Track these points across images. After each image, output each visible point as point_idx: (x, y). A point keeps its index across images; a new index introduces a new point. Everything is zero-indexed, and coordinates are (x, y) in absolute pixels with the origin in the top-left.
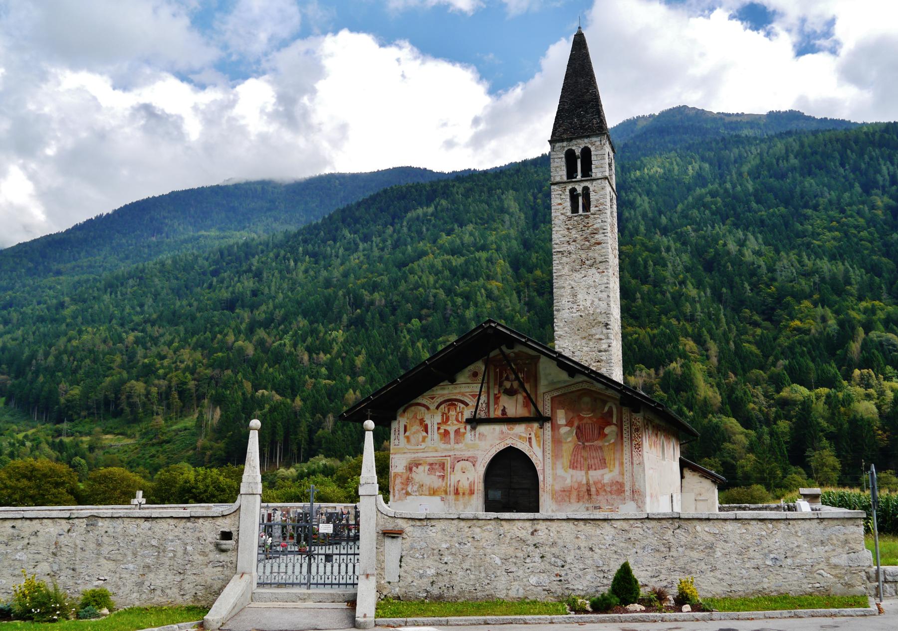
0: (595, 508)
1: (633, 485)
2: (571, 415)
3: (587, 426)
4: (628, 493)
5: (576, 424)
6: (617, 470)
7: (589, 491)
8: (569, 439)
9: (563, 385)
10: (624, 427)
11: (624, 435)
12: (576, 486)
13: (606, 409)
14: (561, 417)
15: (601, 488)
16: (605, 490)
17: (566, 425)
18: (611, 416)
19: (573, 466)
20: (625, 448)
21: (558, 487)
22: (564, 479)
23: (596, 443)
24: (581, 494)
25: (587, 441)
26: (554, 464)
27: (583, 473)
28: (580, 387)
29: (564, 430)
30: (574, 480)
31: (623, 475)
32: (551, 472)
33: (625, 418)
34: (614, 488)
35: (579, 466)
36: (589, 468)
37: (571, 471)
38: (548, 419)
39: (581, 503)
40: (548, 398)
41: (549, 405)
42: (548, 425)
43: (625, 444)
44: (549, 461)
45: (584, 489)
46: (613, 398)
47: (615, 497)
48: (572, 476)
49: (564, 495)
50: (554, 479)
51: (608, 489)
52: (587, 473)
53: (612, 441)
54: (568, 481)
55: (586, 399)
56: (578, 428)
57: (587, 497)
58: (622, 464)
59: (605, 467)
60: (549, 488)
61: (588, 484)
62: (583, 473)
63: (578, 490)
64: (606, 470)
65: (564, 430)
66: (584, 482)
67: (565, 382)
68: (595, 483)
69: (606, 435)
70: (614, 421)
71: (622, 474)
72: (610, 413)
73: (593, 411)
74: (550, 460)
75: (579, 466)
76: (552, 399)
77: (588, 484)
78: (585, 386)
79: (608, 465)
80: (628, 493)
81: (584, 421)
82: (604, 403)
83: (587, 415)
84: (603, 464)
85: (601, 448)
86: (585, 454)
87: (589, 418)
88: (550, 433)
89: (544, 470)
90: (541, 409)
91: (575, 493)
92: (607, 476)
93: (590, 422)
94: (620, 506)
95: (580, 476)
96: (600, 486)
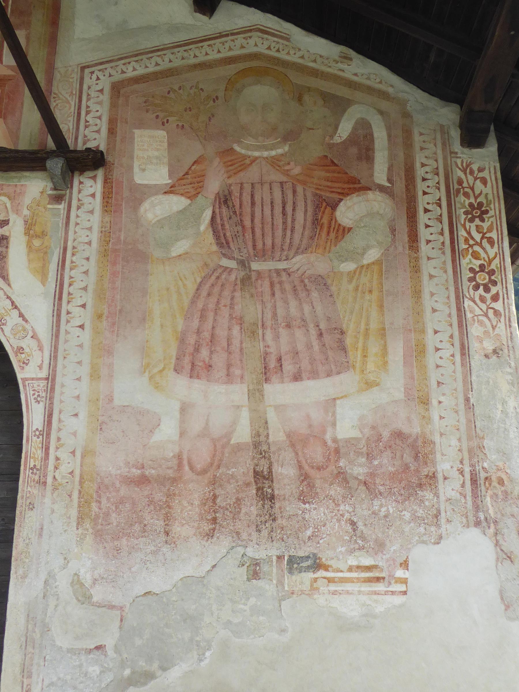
0: (294, 564)
1: (476, 451)
2: (194, 149)
3: (262, 194)
4: (450, 489)
5: (214, 185)
6: (394, 385)
7: (263, 478)
8: (181, 247)
9: (168, 40)
10: (422, 202)
11: (424, 234)
12: (202, 455)
13: (345, 129)
14: (150, 158)
15: (325, 466)
16: (342, 477)
17: (171, 190)
18: (367, 155)
19: (193, 360)
20: (428, 287)
21: (111, 463)
22: (148, 422)
23: (298, 262)
24: (227, 495)
25: (262, 254)
26: (103, 351)
27: (238, 393)
28: (236, 47)
29: (159, 209)
30: (196, 426)
31: (425, 402)
32: (84, 388)
33: (426, 161)
34: (386, 463)
35: (219, 360)
36: (269, 370)
37: (183, 387)
38: (91, 161)
39: (223, 543)
40: (99, 83)
41: (104, 111)
42: (89, 188)
43: (428, 268)
44: (78, 339)
45: (243, 468)
46: (370, 90)
47: (390, 507)
48: (185, 409)
49: (137, 504)
50: (99, 426)
51: (359, 470)
52: (256, 395)
53: (373, 255)
54: (168, 431)
55: (261, 92)
56: (224, 199)
57: (251, 509)
58: (417, 352)
59: (344, 367)
60: (66, 464)
61: (259, 446)
62: (238, 393)
63: (212, 473)
64: (347, 381)
65: (159, 209)
66: (243, 434)
67: (174, 28)
68: (295, 441)
69: (343, 231)
70: (380, 176)
71: (420, 399)
72: (362, 144)
73: (289, 137)
74: (86, 337)
75: (219, 360)
76: (117, 88)
77: (259, 446)
78: (256, 45)
79: (355, 356)
80: (450, 489)
81: (253, 174)
82: (338, 105)
83: (260, 150)
84: (334, 349)
85: (322, 282)
86: (250, 309)
87: (274, 162)
88: (96, 220)
89: (51, 379)
90: (66, 126)
91: (195, 491)
92: (349, 407)
93: (276, 177)
94: (418, 553)
95: (222, 406)
96: (317, 454)
